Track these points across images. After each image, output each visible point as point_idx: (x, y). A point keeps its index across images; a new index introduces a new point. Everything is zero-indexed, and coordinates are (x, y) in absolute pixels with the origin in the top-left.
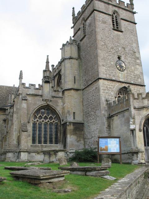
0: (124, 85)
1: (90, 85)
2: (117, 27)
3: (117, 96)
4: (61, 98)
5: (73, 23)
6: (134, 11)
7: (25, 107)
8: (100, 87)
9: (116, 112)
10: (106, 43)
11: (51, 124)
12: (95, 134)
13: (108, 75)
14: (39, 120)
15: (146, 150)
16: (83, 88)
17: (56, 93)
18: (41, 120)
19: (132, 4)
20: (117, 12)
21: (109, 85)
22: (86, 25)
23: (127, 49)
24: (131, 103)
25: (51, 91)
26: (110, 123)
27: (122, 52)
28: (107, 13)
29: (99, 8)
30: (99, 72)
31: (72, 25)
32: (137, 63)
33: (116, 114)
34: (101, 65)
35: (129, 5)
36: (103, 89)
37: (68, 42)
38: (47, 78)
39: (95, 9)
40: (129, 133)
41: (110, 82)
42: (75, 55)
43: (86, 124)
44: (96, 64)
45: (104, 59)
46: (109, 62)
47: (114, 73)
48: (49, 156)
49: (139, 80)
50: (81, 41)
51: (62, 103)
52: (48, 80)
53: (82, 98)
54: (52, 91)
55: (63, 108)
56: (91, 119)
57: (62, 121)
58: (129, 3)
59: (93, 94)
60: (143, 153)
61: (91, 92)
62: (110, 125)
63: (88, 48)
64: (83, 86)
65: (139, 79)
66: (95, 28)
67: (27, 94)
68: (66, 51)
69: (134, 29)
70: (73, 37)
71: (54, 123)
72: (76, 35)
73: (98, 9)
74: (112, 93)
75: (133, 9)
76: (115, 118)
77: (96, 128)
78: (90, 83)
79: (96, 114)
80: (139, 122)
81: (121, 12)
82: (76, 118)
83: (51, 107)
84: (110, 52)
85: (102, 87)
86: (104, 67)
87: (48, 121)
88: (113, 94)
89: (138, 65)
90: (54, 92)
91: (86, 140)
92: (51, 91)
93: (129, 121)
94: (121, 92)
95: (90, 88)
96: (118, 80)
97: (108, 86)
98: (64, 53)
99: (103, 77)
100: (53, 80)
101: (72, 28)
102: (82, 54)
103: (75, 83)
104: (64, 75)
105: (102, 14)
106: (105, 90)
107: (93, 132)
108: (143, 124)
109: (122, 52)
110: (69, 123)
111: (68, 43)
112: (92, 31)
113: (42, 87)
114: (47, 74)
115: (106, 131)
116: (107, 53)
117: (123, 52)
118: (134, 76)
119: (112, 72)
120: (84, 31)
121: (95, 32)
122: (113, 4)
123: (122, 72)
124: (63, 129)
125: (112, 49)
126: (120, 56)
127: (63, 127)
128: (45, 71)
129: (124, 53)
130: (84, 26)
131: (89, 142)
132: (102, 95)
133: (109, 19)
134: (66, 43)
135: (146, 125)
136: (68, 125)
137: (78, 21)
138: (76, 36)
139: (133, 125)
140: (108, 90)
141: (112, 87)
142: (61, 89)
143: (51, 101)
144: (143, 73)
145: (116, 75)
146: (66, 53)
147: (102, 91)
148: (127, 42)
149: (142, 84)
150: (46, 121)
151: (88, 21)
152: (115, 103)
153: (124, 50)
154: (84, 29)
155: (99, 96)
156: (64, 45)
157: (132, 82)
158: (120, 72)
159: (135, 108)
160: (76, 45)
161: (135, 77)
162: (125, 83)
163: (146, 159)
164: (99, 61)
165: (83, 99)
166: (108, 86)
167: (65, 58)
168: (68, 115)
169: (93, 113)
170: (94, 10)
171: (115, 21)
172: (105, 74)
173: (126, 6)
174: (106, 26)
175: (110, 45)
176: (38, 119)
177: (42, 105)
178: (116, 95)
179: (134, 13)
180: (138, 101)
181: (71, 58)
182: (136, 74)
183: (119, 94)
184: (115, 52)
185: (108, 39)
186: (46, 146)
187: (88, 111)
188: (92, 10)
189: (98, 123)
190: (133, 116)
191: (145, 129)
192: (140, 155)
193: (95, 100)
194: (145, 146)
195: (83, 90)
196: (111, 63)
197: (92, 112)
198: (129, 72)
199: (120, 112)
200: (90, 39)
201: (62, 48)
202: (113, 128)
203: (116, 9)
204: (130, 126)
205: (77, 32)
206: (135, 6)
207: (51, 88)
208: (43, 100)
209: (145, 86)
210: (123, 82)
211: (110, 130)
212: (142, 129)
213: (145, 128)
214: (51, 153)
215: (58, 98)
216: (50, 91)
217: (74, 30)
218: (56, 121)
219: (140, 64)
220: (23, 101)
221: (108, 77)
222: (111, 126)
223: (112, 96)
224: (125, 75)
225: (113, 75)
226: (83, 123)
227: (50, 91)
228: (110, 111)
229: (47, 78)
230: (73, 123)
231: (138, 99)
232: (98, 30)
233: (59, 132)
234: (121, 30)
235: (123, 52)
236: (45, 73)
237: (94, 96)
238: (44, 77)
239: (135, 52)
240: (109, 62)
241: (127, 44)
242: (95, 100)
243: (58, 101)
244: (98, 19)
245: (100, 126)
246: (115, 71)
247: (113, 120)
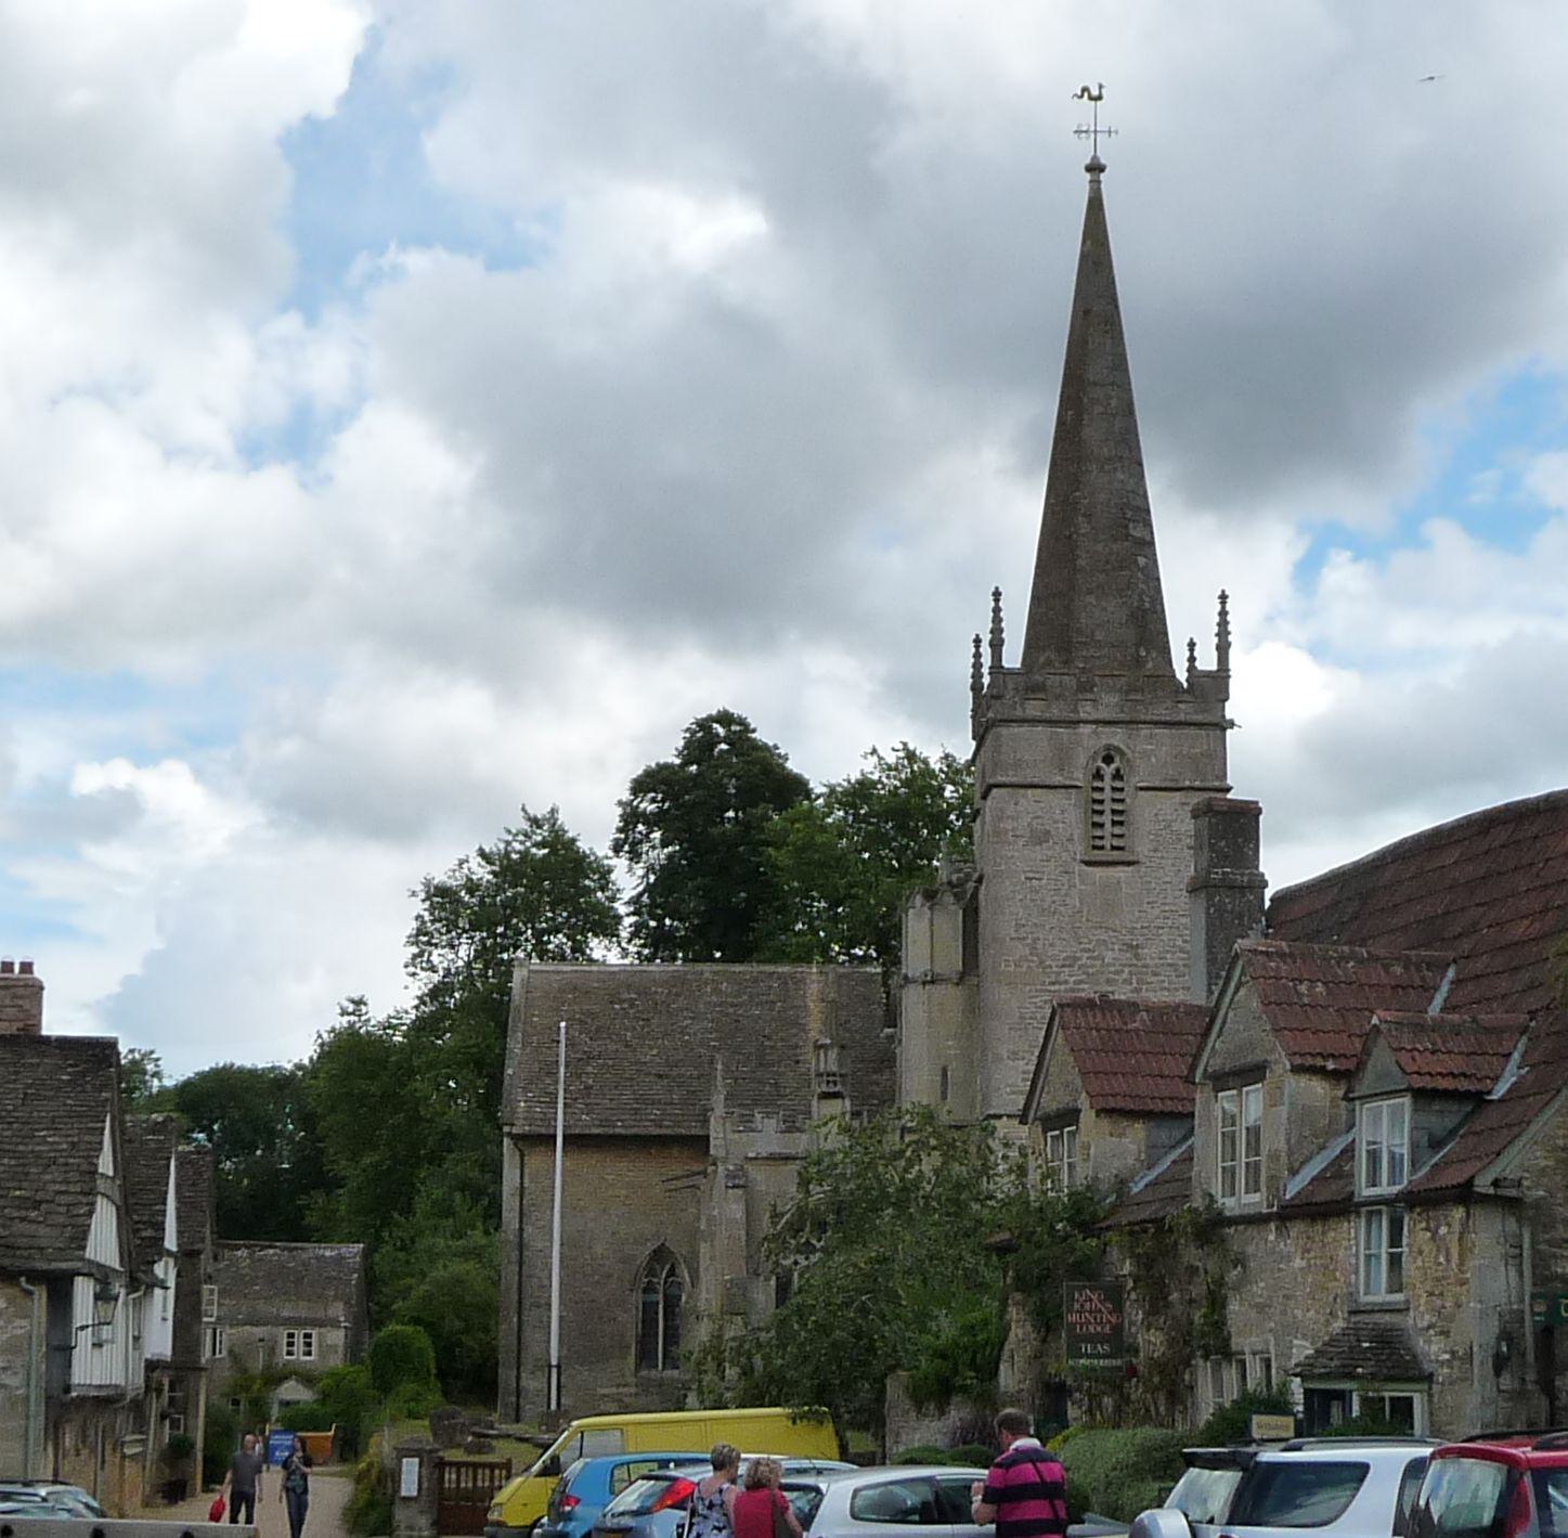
7: (738, 1216)
19: (1221, 677)
27: (1117, 973)
28: (1058, 779)
29: (1017, 765)
38: (828, 1082)
39: (992, 781)
42: (953, 960)
67: (747, 1158)
75: (1227, 699)
84: (1053, 983)
105: (1030, 792)
116: (1042, 991)
117: (1126, 970)
125: (1070, 966)
129: (1130, 973)
133: (1065, 814)
148: (1156, 912)
153: (1137, 956)
160: (953, 908)
170: (990, 787)
174: (1050, 853)
179: (1232, 724)
181: (933, 980)
185: (1054, 921)
203: (1116, 737)
206: (1234, 686)
220: (730, 1191)
241: (1159, 922)
244: (1007, 831)
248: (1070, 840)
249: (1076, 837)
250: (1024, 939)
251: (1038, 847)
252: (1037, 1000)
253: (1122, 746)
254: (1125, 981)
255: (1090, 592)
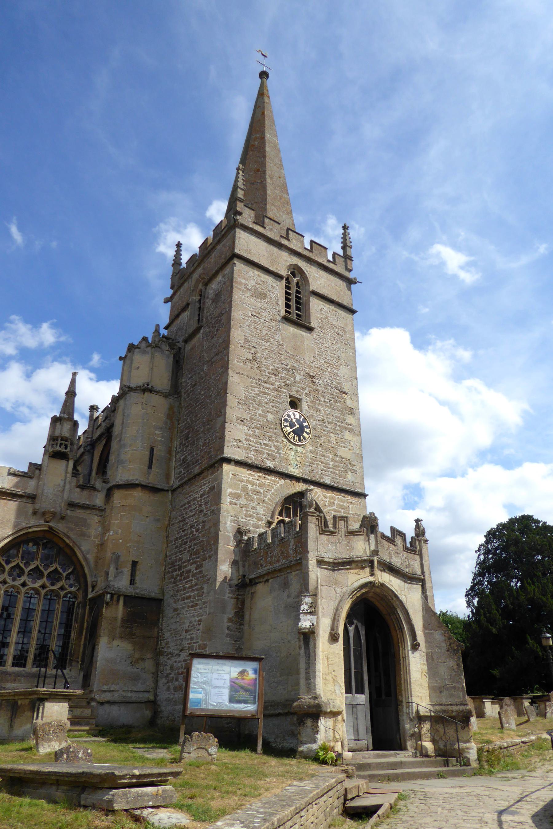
0: (300, 487)
1: (195, 477)
2: (297, 315)
3: (276, 521)
4: (98, 513)
5: (171, 288)
6: (351, 275)
8: (224, 485)
9: (267, 568)
10: (259, 355)
11: (52, 596)
12: (192, 639)
13: (254, 450)
14: (9, 580)
15: (351, 706)
16: (175, 486)
17: (85, 492)
18: (18, 583)
19: (347, 258)
20: (302, 272)
21: (253, 484)
22: (208, 297)
23: (321, 382)
24: (311, 545)
25: (67, 486)
26: (243, 603)
27: (303, 389)
29: (249, 251)
30: (224, 441)
31: (170, 292)
32: (347, 424)
33: (264, 578)
34: (235, 418)
35: (338, 259)
36: (232, 495)
37: (145, 339)
38: (61, 444)
39: (237, 251)
40: (296, 642)
41: (255, 476)
43: (169, 603)
44: (220, 416)
45: (245, 402)
46: (260, 412)
47: (273, 448)
48: (10, 715)
49: (350, 477)
50: (186, 341)
51: (100, 529)
52: (62, 449)
53: (167, 519)
54: (73, 484)
55: (102, 545)
56: (185, 589)
57: (90, 589)
58: (341, 252)
59: (200, 506)
60: (340, 718)
61: (194, 499)
62: (243, 612)
63: (204, 364)
64: (176, 479)
65: (350, 473)
66: (230, 307)
68: (135, 365)
69: (346, 325)
70: (166, 328)
71: (62, 593)
72: (175, 324)
73: (245, 255)
74: (261, 510)
75: (350, 271)
76: (261, 588)
77: (197, 619)
78: (197, 470)
79: (201, 572)
80: (331, 611)
81: (311, 271)
82: (138, 578)
83: (62, 539)
85: (230, 486)
86: (241, 427)
87: (43, 587)
88: (262, 512)
89: (351, 431)
90: (78, 490)
91: (163, 659)
92: (67, 486)
93: (299, 603)
94: (288, 509)
95: (193, 488)
96: (284, 470)
97: (250, 487)
98: (130, 371)
99: (237, 457)
100: (89, 451)
101: (166, 301)
102: (185, 382)
103: (150, 467)
104: (120, 440)
106: (238, 496)
107: (187, 631)
108: (344, 614)
109: (303, 389)
110: (112, 595)
111: (144, 342)
112: (222, 314)
113: (40, 470)
114: (65, 430)
115: (227, 632)
117: (307, 389)
118: (336, 461)
119: (265, 444)
120: (199, 315)
121: (229, 319)
122: (292, 246)
123: (299, 449)
124: (90, 613)
125: (276, 375)
126: (298, 399)
127: (91, 609)
128: (55, 420)
130: (200, 300)
131: (172, 668)
132: (228, 511)
134: (140, 342)
135: (355, 622)
136: (107, 604)
137: (185, 281)
138: (174, 328)
139: (309, 617)
140: (249, 498)
141: (262, 491)
142: (104, 482)
143: (63, 518)
144: (362, 457)
145: (278, 455)
146: (134, 372)
147: (226, 500)
149: (358, 490)
150: (37, 585)
151: (214, 286)
152: (266, 539)
153: (312, 382)
154: (200, 308)
155: (217, 513)
156: (132, 348)
157: (327, 480)
158: (293, 447)
159: (320, 562)
160: (167, 352)
161: (337, 467)
162: (305, 481)
163: (349, 741)
164: (231, 408)
165: (170, 520)
166: (250, 487)
167: (129, 387)
168: (112, 570)
169: (193, 568)
171: (293, 297)
172: (245, 448)
173: (330, 258)
174: (266, 306)
175: (269, 365)
176: (6, 575)
177: (30, 528)
178: (272, 517)
180: (332, 539)
181: (146, 389)
182: (341, 457)
183: (280, 514)
184: (283, 384)
186: (19, 675)
187: (181, 559)
188: (229, 255)
189: (204, 603)
190: (311, 587)
191: (351, 635)
192: (323, 723)
193: (203, 527)
194: (348, 690)
195: (174, 491)
196: (266, 417)
197: (192, 564)
198: (319, 448)
199: (275, 571)
200: (212, 338)
201: (126, 356)
202: (250, 621)
204: (299, 620)
205: (177, 316)
206: (355, 264)
207: (69, 476)
208: (35, 513)
209: (364, 496)
210: (298, 479)
211: (240, 630)
212: (341, 631)
213: (351, 629)
214: (19, 703)
215: (89, 511)
216: (64, 486)
217: (172, 307)
218: (71, 586)
219: (357, 429)
221: (252, 457)
222: (247, 617)
223: (259, 519)
224: (305, 457)
225: (268, 454)
226: (161, 600)
227: (64, 486)
228: (247, 564)
229: (59, 442)
230: (126, 596)
231: (333, 533)
232: (236, 314)
233: (75, 625)
234: (310, 323)
235: (307, 389)
236: (58, 425)
237: (203, 513)
238: (52, 439)
239: (346, 393)
240: (260, 412)
242: (203, 527)
243: (88, 521)
245: (209, 614)
246: (277, 442)
247: (253, 594)
248: (277, 304)
249: (280, 303)
250: (250, 349)
251: (259, 300)
252: (257, 389)
253: (303, 269)
254: (306, 395)
255: (272, 204)
